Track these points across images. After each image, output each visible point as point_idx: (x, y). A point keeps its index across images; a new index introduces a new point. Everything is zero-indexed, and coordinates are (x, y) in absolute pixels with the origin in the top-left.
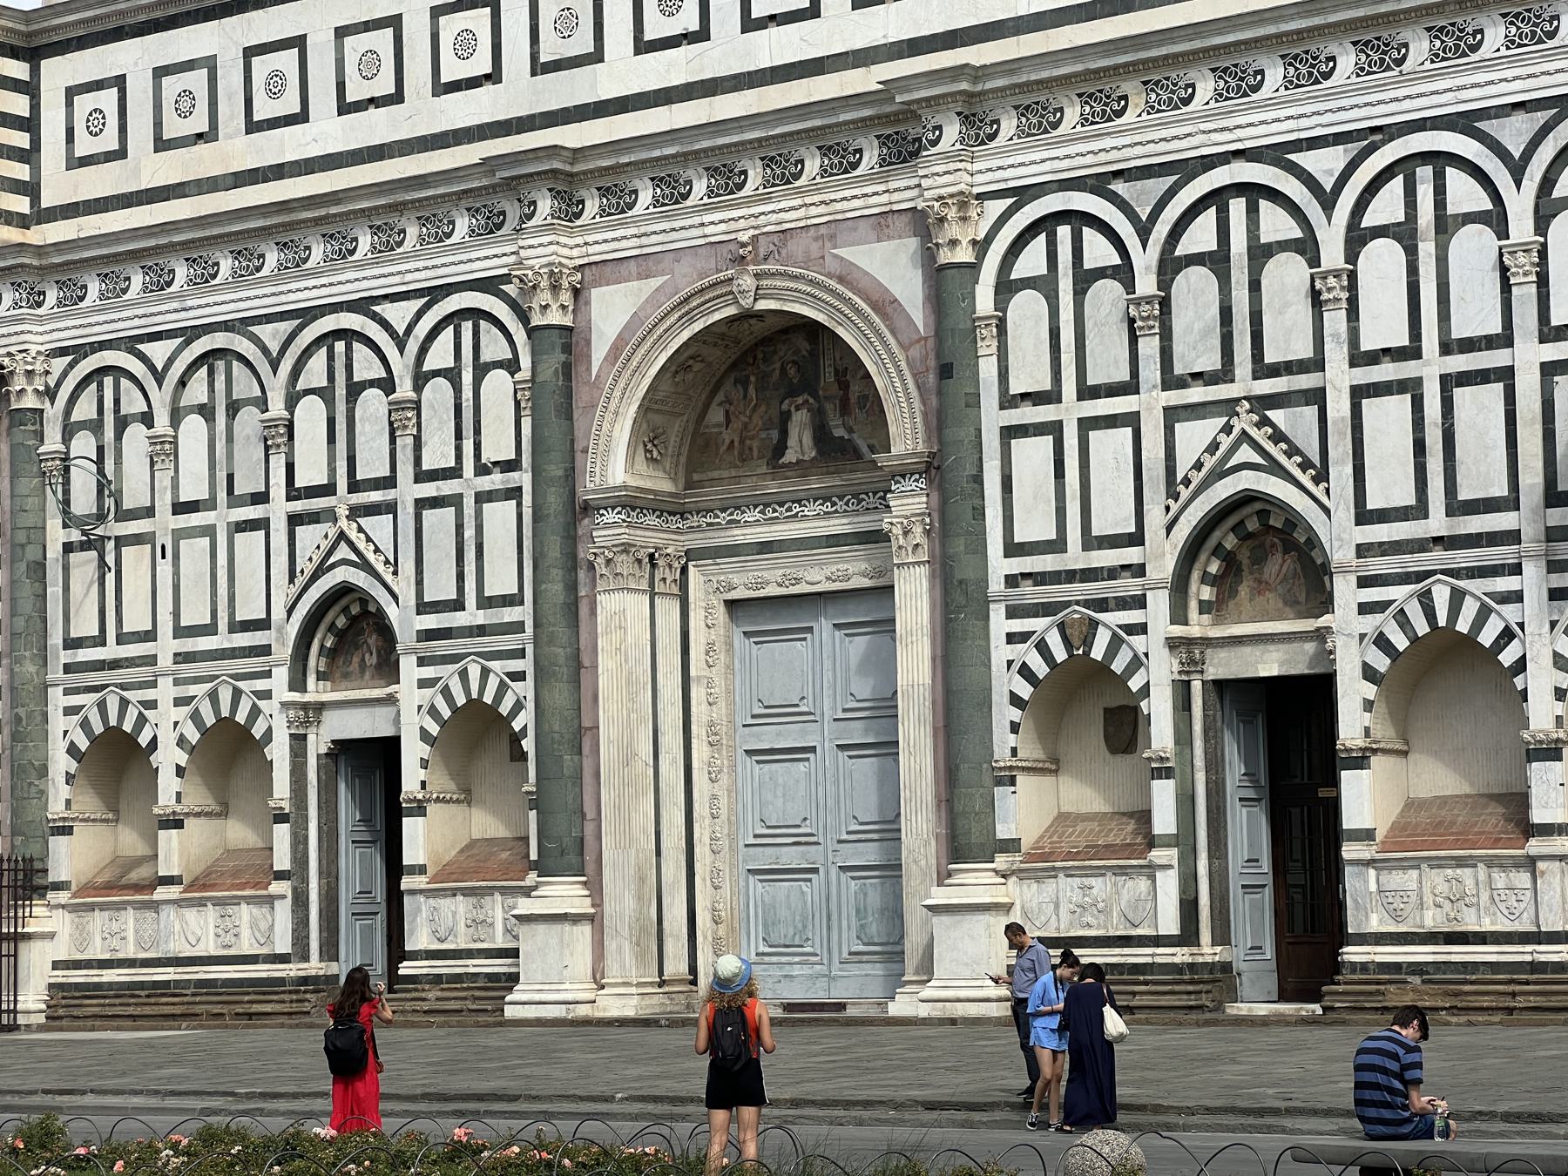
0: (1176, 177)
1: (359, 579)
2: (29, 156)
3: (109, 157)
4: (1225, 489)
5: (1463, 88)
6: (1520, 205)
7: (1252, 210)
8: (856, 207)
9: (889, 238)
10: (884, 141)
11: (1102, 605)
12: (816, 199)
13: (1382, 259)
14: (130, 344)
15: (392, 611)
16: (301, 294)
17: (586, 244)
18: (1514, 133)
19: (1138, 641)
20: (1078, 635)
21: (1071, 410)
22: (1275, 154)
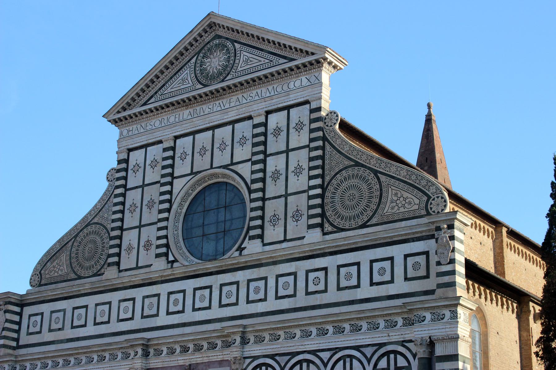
0: (290, 356)
2: (18, 332)
5: (357, 339)
7: (308, 366)
8: (215, 359)
9: (222, 367)
10: (223, 341)
12: (205, 355)
17: (149, 363)
18: (368, 351)
22: (313, 352)
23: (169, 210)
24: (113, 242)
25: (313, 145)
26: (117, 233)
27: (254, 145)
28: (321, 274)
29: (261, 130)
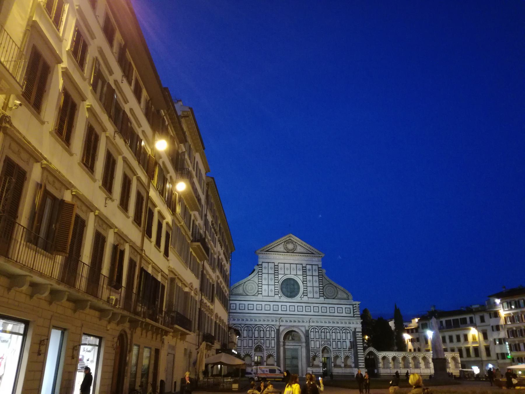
1: (260, 344)
3: (234, 309)
4: (325, 346)
6: (341, 332)
11: (317, 352)
13: (334, 334)
14: (240, 324)
15: (264, 347)
16: (256, 323)
19: (319, 354)
20: (316, 354)
21: (315, 340)
22: (328, 327)
23: (278, 282)
24: (259, 287)
25: (320, 276)
26: (261, 285)
27: (303, 272)
28: (325, 308)
29: (305, 268)
